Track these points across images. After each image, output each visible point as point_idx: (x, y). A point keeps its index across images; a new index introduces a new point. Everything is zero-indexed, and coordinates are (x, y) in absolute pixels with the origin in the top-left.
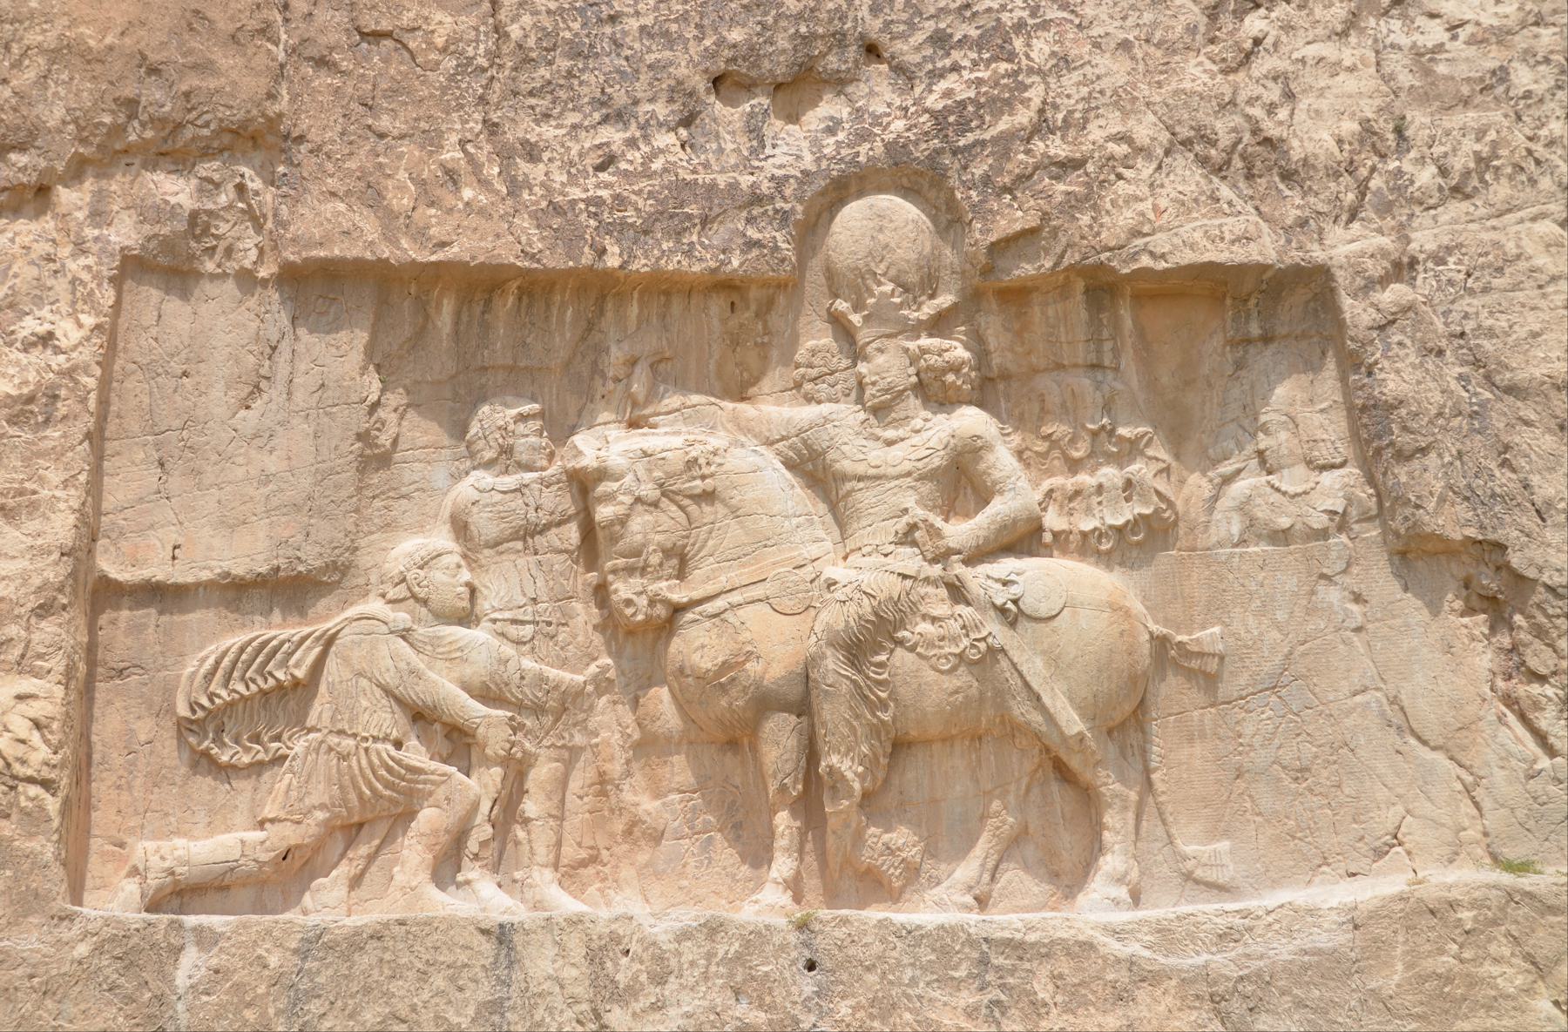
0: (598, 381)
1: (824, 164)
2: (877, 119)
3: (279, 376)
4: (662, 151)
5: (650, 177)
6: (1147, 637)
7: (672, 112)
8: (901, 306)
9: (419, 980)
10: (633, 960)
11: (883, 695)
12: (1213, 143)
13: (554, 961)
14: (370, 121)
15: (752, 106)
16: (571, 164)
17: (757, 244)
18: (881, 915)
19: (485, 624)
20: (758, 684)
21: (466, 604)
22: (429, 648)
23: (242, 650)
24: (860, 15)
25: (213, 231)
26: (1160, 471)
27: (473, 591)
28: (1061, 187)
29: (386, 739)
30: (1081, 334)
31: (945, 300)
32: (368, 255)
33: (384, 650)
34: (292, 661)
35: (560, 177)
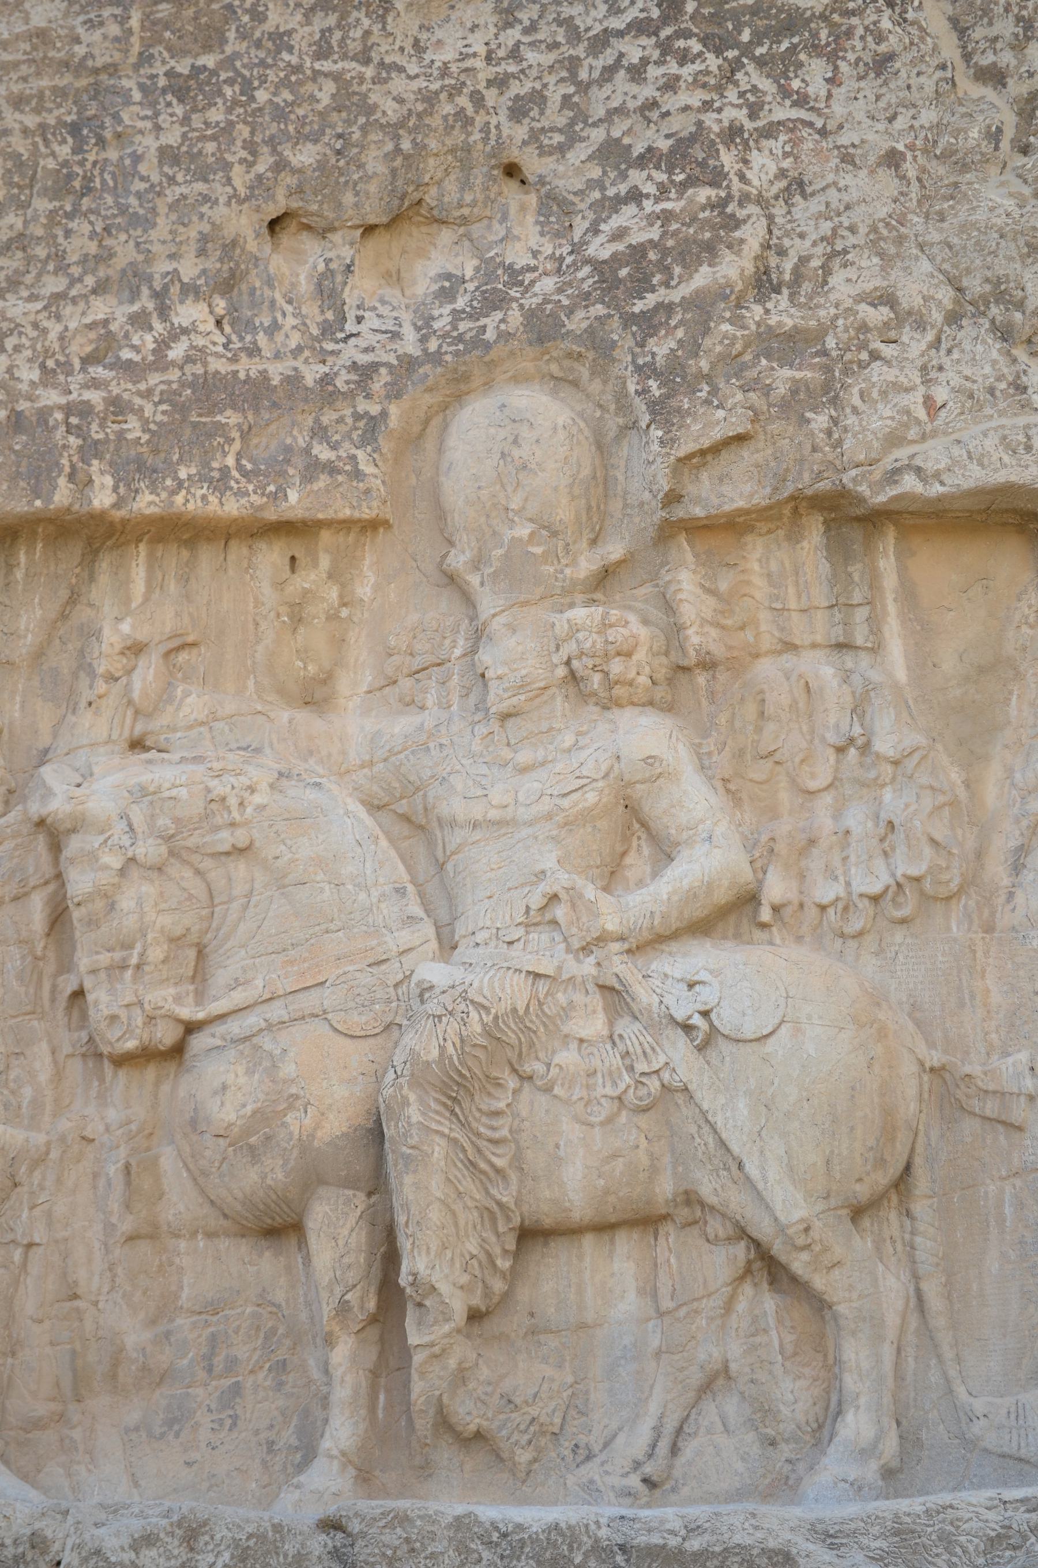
0: (84, 681)
1: (433, 345)
2: (514, 275)
4: (185, 331)
5: (164, 369)
6: (915, 1068)
7: (204, 272)
8: (545, 557)
11: (499, 1162)
12: (1020, 305)
15: (328, 261)
16: (48, 353)
17: (331, 469)
18: (460, 1509)
20: (305, 1146)
24: (494, 121)
26: (939, 808)
28: (786, 373)
30: (820, 596)
31: (614, 550)
35: (29, 374)
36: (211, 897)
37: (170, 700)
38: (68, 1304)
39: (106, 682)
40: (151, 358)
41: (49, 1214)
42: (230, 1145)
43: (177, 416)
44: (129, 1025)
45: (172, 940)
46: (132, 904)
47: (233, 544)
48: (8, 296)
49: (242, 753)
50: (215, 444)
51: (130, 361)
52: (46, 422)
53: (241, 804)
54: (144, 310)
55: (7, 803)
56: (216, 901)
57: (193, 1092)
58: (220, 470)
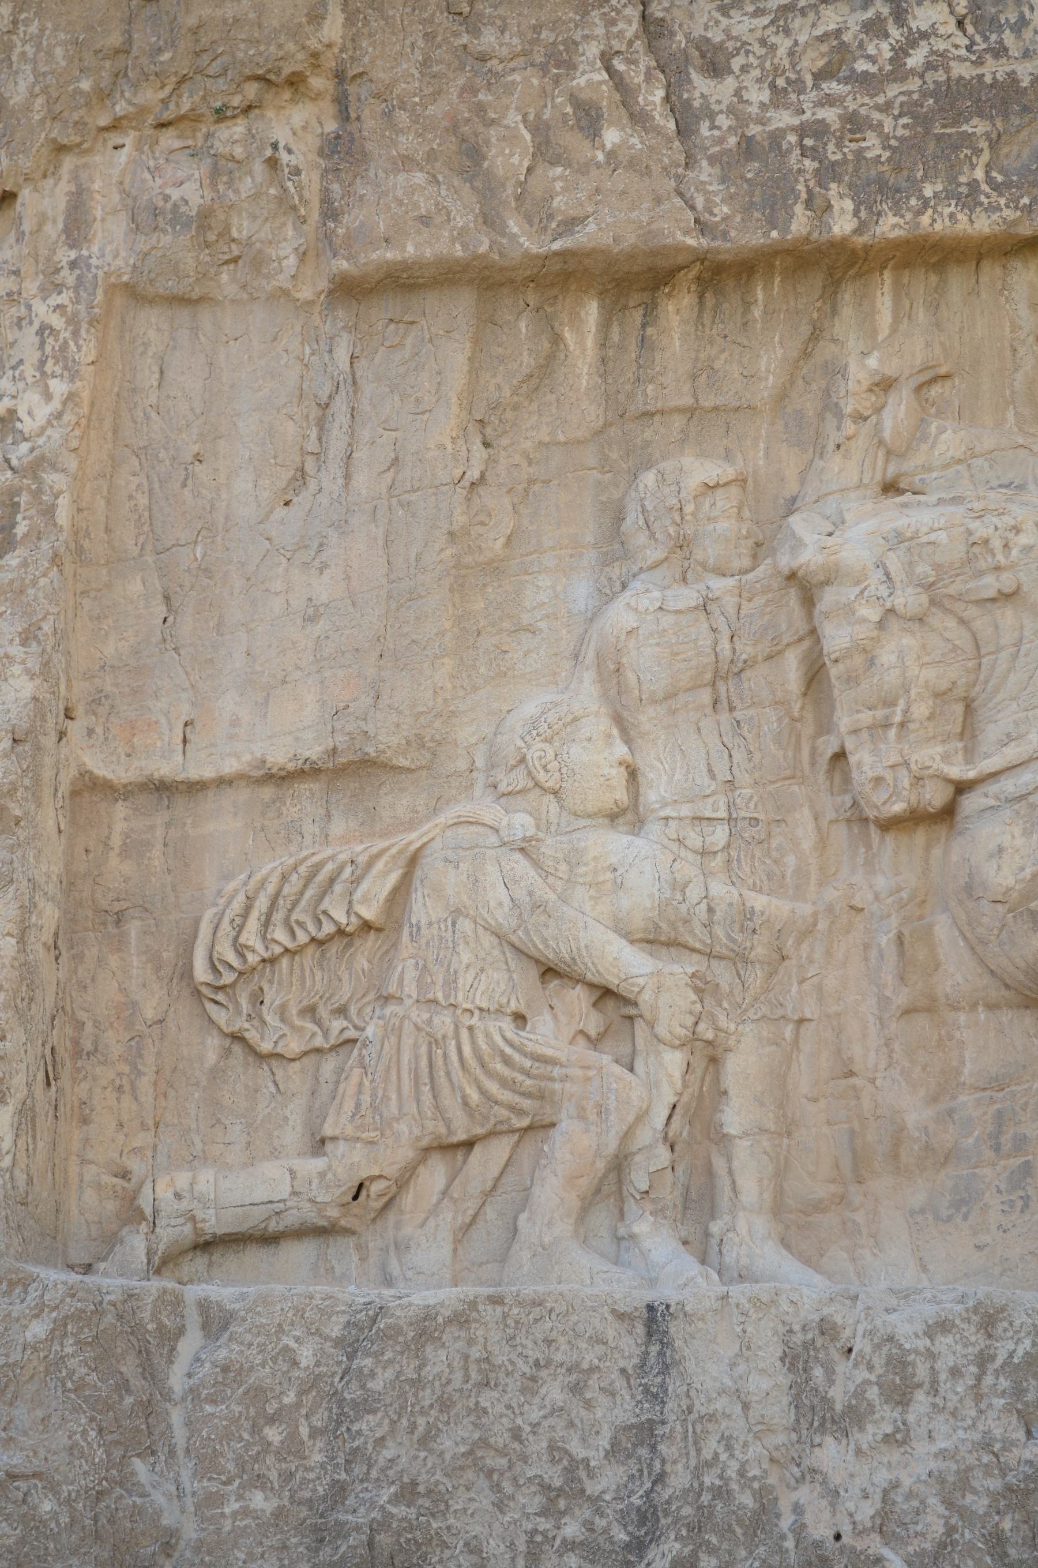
0: (831, 422)
3: (331, 455)
4: (924, 35)
5: (903, 79)
9: (523, 1390)
10: (856, 1365)
13: (733, 1365)
14: (465, 39)
19: (654, 828)
21: (621, 795)
22: (563, 867)
23: (284, 878)
25: (235, 234)
27: (633, 774)
29: (499, 1011)
32: (458, 251)
33: (492, 874)
34: (358, 895)
35: (758, 95)
36: (978, 647)
37: (924, 438)
38: (844, 1082)
39: (855, 422)
40: (889, 68)
41: (819, 989)
42: (1009, 911)
43: (919, 129)
44: (895, 786)
45: (937, 695)
46: (893, 658)
47: (986, 265)
48: (732, 12)
49: (1004, 491)
50: (962, 156)
51: (866, 73)
52: (779, 146)
53: (1006, 546)
54: (878, 15)
55: (755, 556)
56: (983, 651)
57: (967, 856)
58: (968, 184)
